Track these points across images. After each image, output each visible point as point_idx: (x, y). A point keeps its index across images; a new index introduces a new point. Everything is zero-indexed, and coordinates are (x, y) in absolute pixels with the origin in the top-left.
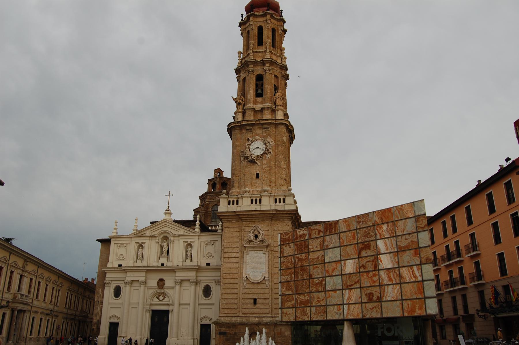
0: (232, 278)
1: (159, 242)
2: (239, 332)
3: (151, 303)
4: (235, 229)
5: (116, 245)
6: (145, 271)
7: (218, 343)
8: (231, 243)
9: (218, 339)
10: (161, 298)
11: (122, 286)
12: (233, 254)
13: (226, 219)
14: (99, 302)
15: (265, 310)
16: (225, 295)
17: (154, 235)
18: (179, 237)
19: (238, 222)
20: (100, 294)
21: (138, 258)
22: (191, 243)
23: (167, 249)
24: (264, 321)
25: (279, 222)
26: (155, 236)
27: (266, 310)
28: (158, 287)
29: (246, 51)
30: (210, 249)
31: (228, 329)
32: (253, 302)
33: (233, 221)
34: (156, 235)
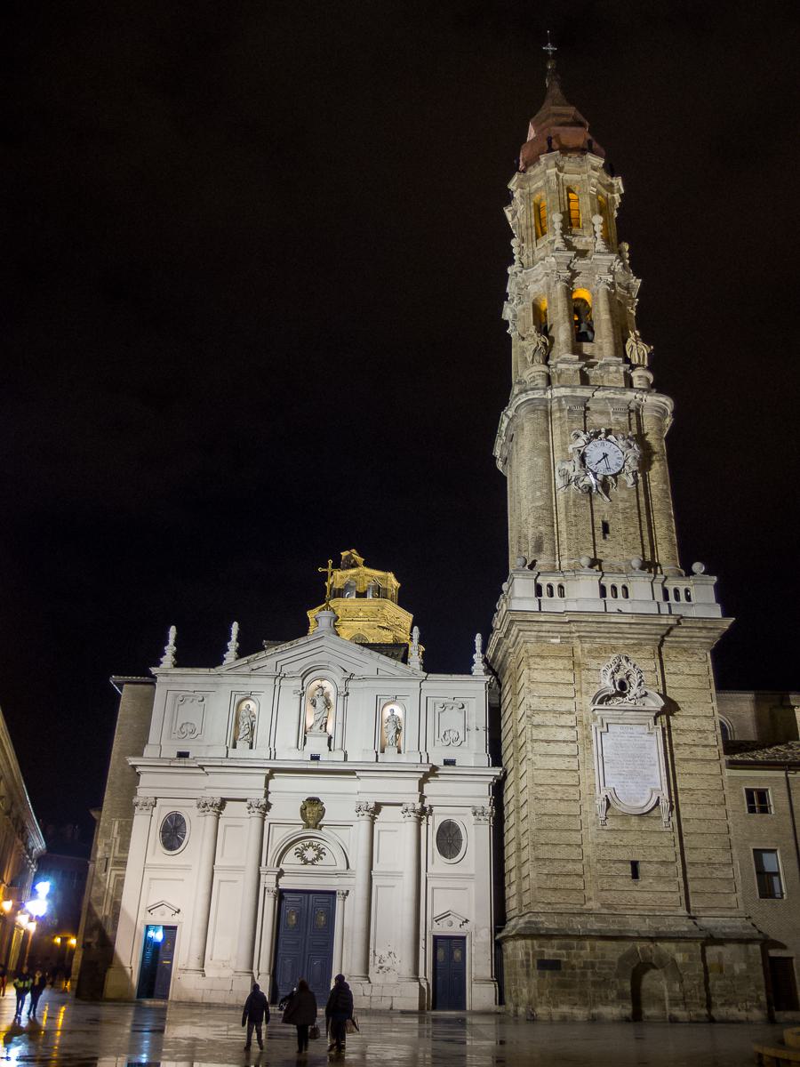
0: (561, 800)
2: (600, 962)
4: (560, 661)
7: (537, 995)
8: (549, 700)
9: (535, 981)
10: (310, 854)
11: (191, 814)
12: (560, 730)
13: (533, 633)
15: (664, 895)
16: (546, 848)
19: (568, 642)
21: (240, 737)
24: (672, 929)
25: (678, 650)
27: (669, 895)
29: (534, 239)
30: (453, 720)
31: (564, 952)
32: (630, 870)
33: (553, 640)
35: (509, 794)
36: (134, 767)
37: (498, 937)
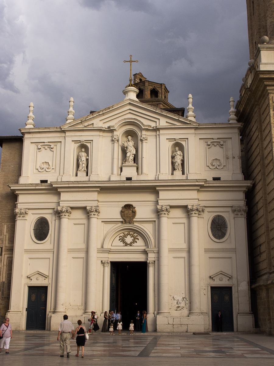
1: (118, 141)
3: (111, 249)
5: (34, 146)
6: (99, 189)
10: (129, 239)
11: (51, 219)
14: (4, 248)
17: (109, 127)
18: (158, 132)
20: (5, 234)
21: (79, 169)
22: (179, 142)
23: (134, 153)
26: (111, 128)
28: (122, 220)
30: (217, 152)
34: (113, 126)
35: (259, 196)
36: (15, 190)
37: (253, 286)
